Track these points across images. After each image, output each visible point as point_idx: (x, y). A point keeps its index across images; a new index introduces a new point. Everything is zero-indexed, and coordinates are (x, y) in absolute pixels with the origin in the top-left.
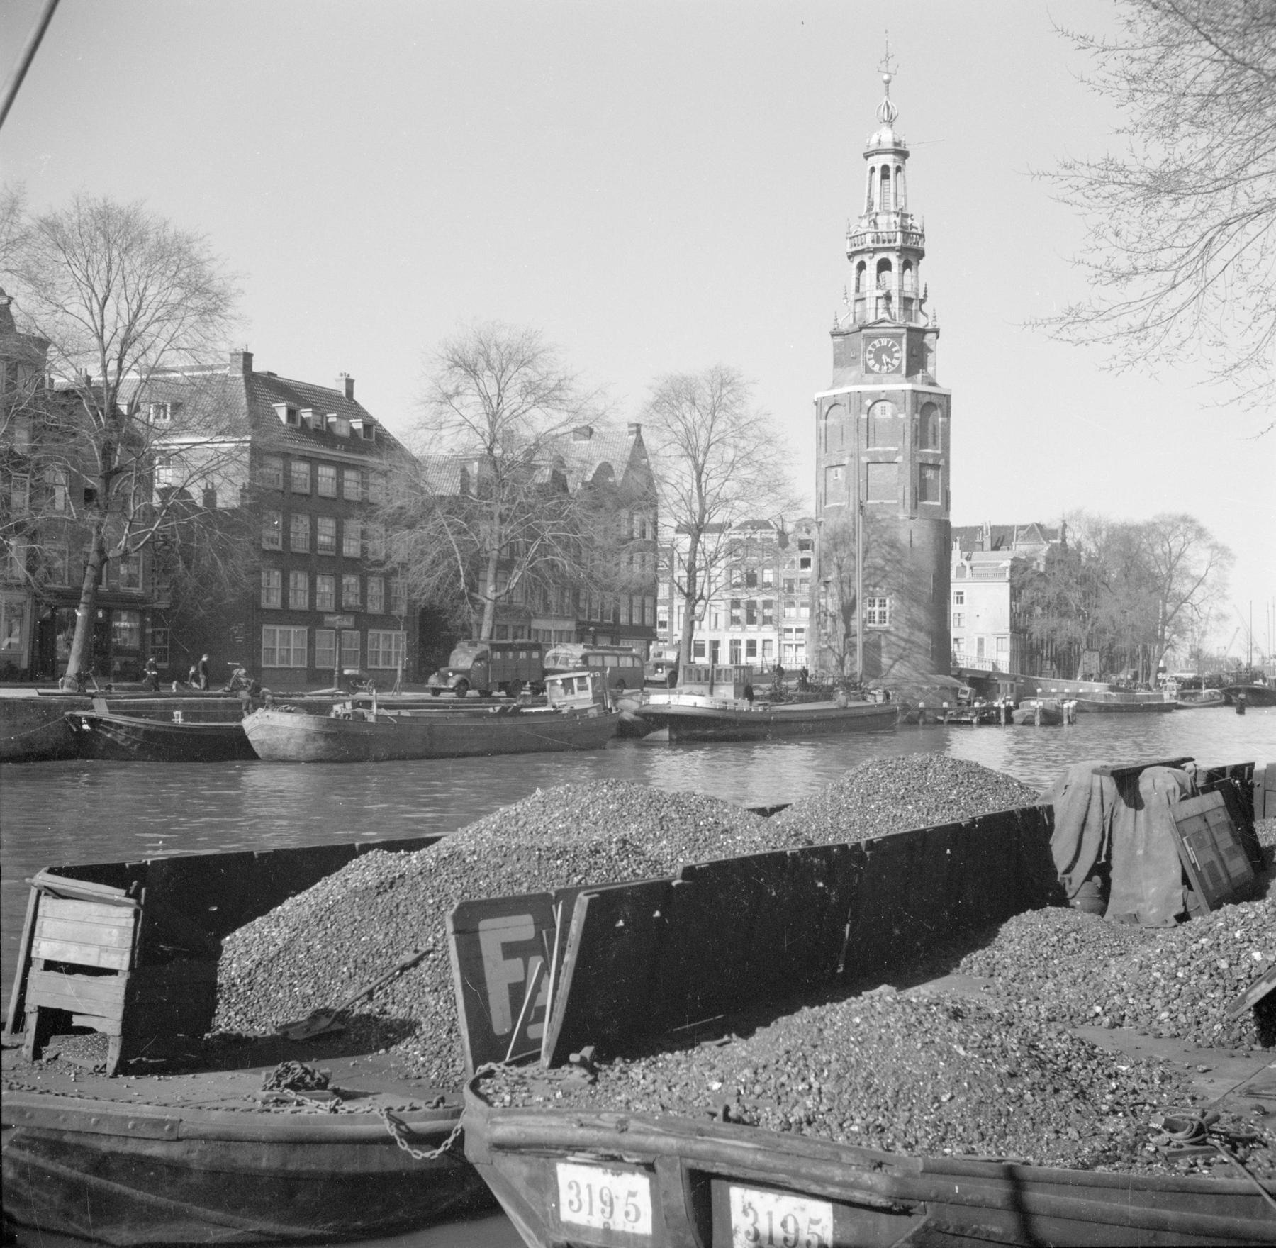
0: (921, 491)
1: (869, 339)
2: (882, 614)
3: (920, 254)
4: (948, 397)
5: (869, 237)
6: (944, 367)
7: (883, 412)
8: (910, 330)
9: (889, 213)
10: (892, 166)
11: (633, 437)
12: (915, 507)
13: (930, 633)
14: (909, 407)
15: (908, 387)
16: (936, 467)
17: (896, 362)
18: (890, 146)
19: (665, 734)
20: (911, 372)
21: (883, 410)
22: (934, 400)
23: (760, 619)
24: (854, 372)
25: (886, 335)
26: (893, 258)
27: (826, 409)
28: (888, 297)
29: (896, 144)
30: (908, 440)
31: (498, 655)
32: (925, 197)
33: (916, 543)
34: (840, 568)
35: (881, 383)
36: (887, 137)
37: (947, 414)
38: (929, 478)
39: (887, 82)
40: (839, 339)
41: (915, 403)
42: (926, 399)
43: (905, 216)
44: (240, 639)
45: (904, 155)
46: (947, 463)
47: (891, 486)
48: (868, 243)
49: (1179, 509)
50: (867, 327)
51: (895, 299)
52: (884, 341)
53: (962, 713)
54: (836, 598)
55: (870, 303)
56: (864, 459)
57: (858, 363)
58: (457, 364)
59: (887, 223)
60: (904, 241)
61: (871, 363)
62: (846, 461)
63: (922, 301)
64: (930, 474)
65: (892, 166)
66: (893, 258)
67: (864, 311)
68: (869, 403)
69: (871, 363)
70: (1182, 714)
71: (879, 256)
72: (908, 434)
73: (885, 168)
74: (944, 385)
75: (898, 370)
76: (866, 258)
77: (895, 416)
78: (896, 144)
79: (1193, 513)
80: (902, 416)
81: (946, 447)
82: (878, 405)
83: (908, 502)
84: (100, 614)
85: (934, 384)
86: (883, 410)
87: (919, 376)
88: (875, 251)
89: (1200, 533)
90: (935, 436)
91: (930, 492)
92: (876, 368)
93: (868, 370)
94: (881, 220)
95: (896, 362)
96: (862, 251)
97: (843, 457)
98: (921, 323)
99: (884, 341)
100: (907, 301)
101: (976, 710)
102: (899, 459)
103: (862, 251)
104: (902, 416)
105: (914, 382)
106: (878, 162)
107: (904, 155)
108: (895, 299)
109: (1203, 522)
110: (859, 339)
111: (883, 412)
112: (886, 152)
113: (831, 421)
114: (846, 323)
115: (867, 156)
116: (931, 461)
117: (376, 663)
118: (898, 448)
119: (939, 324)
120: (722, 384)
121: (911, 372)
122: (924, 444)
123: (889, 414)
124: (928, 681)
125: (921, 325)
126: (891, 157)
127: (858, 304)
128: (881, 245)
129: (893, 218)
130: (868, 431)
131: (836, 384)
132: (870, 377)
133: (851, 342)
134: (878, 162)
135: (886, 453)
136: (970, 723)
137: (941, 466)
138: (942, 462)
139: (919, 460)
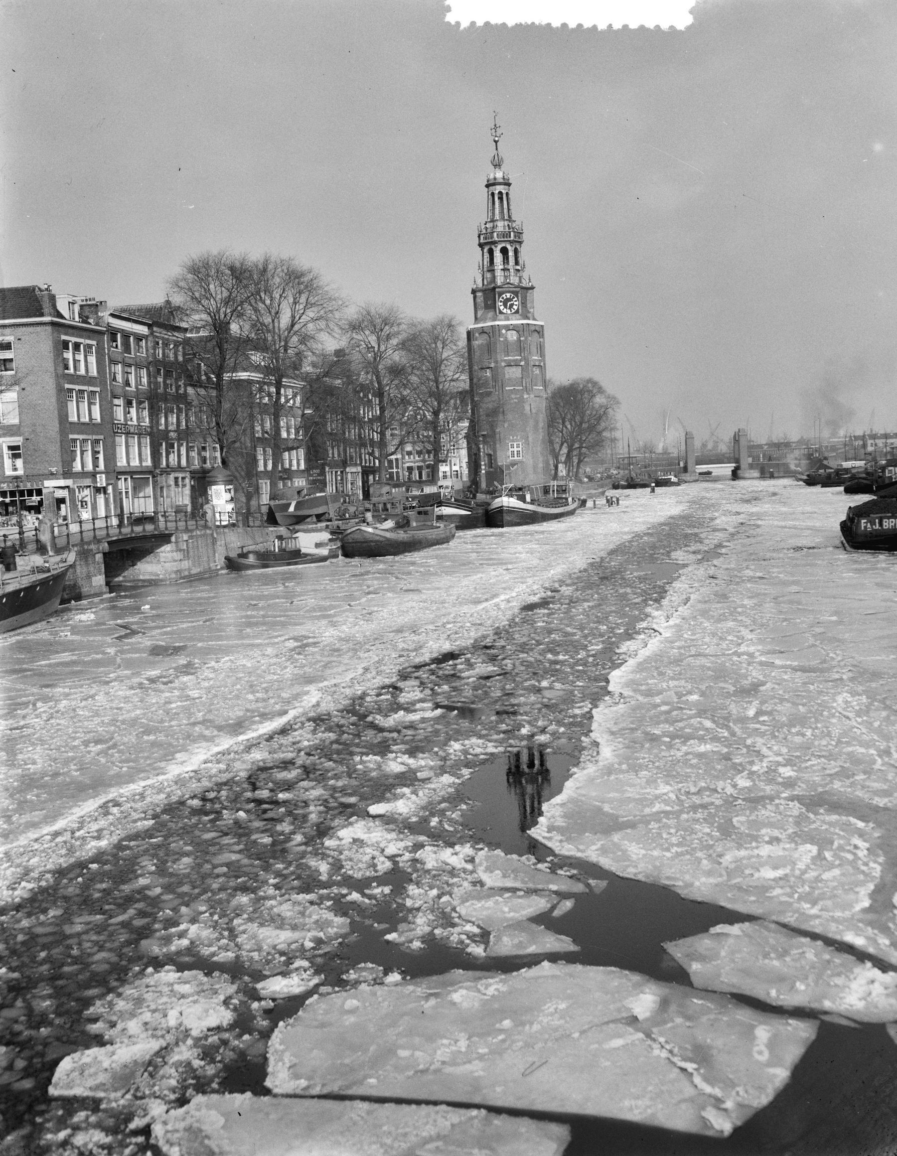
1: (500, 294)
2: (518, 452)
45: (509, 185)
52: (508, 295)
55: (499, 274)
56: (503, 364)
62: (492, 365)
71: (503, 245)
81: (542, 355)
99: (508, 295)
107: (509, 185)
112: (500, 184)
132: (502, 316)
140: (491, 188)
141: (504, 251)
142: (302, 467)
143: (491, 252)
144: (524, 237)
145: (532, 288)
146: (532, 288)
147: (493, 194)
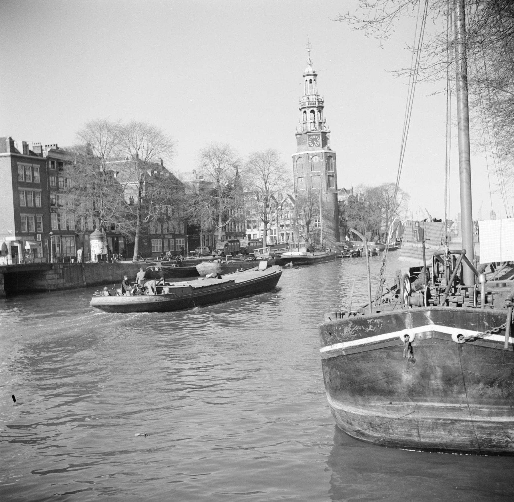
0: (329, 185)
1: (309, 136)
3: (323, 107)
4: (335, 153)
5: (307, 103)
7: (316, 160)
8: (322, 132)
9: (313, 95)
10: (313, 79)
13: (334, 230)
14: (324, 158)
15: (323, 151)
16: (333, 176)
17: (318, 143)
18: (312, 73)
19: (291, 264)
21: (316, 159)
22: (331, 155)
23: (252, 227)
24: (305, 147)
25: (315, 135)
28: (314, 122)
29: (314, 72)
30: (324, 168)
31: (230, 244)
32: (323, 89)
33: (328, 201)
34: (304, 210)
35: (314, 150)
36: (310, 70)
37: (335, 159)
38: (331, 179)
39: (309, 52)
42: (328, 155)
44: (146, 244)
45: (316, 75)
46: (336, 175)
47: (319, 184)
48: (307, 105)
52: (314, 137)
53: (346, 254)
54: (304, 220)
55: (309, 124)
56: (311, 175)
57: (306, 144)
58: (206, 156)
59: (312, 99)
60: (319, 104)
62: (305, 176)
63: (324, 123)
64: (331, 179)
67: (307, 127)
68: (311, 157)
69: (310, 144)
71: (312, 109)
72: (324, 166)
73: (311, 80)
75: (319, 146)
76: (306, 110)
77: (319, 161)
78: (314, 72)
80: (322, 161)
81: (335, 170)
83: (325, 188)
84: (115, 239)
85: (330, 150)
86: (316, 159)
87: (326, 147)
88: (309, 107)
91: (331, 184)
92: (312, 145)
93: (310, 146)
96: (305, 108)
97: (303, 175)
98: (324, 130)
99: (314, 137)
101: (351, 253)
102: (322, 174)
103: (305, 108)
104: (322, 161)
105: (324, 149)
106: (308, 78)
107: (316, 75)
110: (306, 135)
112: (311, 75)
113: (298, 163)
115: (304, 76)
116: (331, 175)
117: (157, 250)
119: (331, 130)
120: (272, 155)
122: (329, 170)
123: (318, 160)
124: (334, 245)
125: (324, 131)
126: (312, 76)
128: (311, 106)
129: (314, 96)
131: (299, 151)
132: (310, 148)
133: (301, 137)
134: (308, 78)
135: (318, 173)
136: (349, 257)
137: (334, 176)
138: (334, 175)
140: (306, 78)
141: (313, 112)
142: (182, 232)
143: (305, 112)
144: (324, 104)
145: (329, 133)
147: (306, 81)
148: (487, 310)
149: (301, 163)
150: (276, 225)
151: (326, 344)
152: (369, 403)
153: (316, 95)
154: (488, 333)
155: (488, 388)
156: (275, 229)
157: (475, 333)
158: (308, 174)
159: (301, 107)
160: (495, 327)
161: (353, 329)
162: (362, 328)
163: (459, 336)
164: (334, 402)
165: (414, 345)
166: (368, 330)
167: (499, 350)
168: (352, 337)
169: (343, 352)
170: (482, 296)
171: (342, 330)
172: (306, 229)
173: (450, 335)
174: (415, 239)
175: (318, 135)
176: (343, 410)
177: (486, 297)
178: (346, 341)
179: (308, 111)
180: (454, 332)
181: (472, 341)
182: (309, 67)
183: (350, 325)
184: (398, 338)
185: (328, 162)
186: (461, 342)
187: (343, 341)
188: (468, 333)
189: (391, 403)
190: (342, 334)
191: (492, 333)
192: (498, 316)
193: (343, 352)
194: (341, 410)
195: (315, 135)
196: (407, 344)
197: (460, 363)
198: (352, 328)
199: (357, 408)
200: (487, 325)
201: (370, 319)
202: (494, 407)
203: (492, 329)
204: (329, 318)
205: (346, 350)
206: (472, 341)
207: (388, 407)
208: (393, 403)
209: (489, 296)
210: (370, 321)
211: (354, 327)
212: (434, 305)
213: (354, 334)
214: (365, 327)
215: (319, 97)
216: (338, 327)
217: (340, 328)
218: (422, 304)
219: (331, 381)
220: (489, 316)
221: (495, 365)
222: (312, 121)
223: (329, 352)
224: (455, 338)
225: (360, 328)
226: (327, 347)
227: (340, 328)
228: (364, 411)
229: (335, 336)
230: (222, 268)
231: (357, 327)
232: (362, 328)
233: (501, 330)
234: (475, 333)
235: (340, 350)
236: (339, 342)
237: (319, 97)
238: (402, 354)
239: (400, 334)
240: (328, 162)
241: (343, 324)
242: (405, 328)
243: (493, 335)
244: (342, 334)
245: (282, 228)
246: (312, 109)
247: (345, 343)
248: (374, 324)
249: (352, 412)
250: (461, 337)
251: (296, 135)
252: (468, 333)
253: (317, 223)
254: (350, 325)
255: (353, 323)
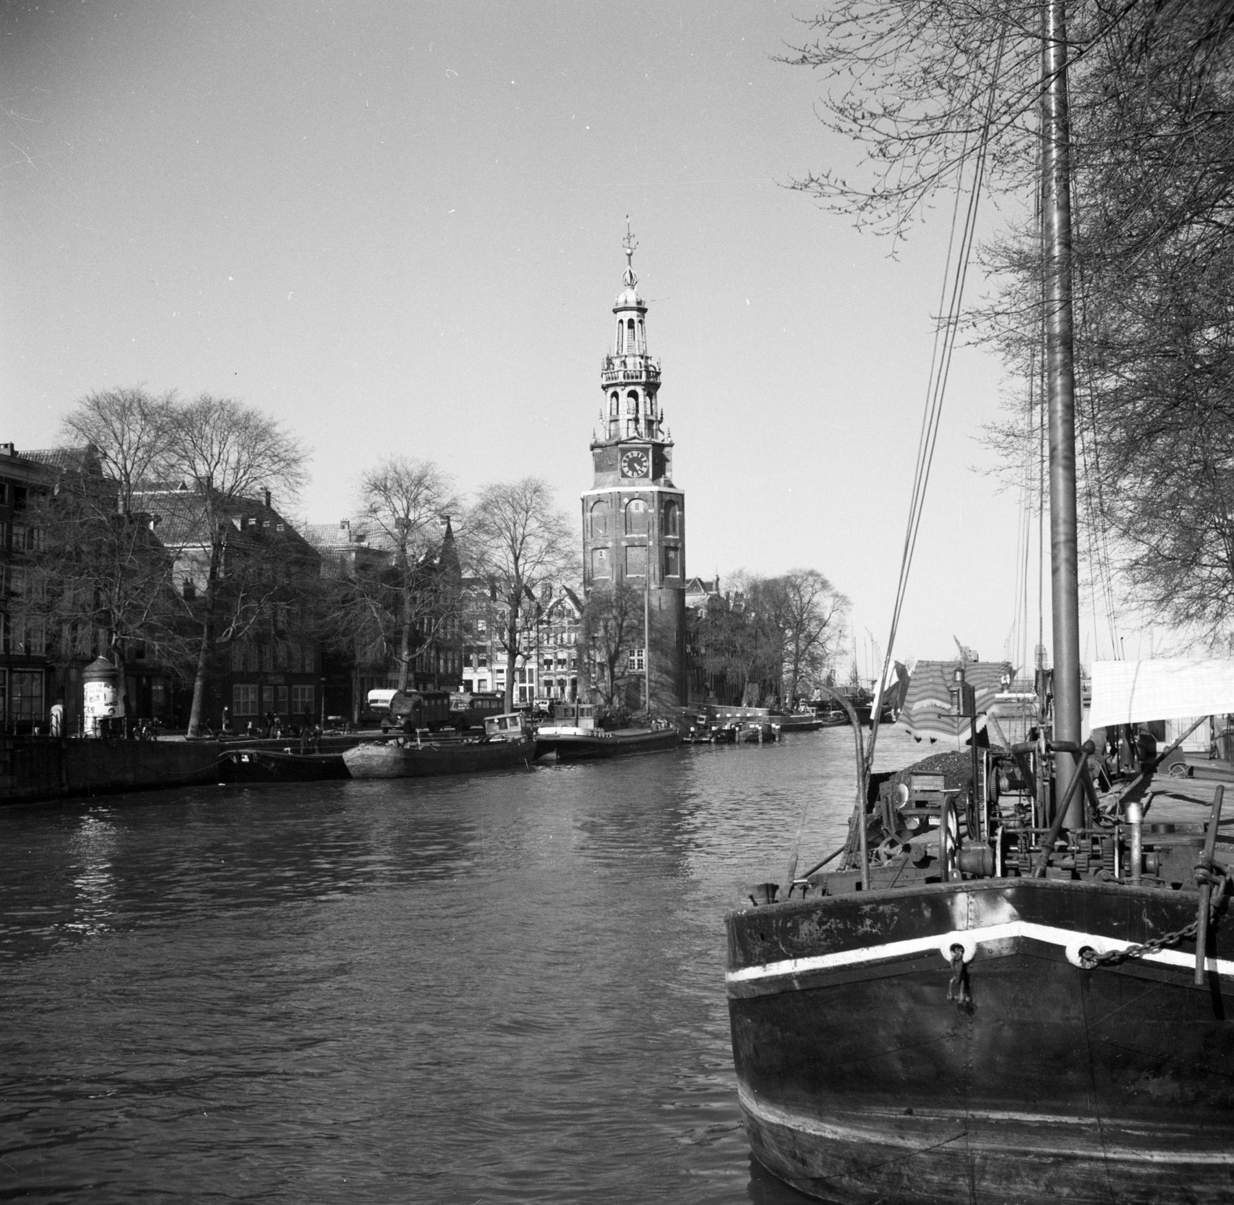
0: (666, 567)
1: (624, 451)
3: (657, 386)
4: (682, 496)
5: (621, 374)
6: (679, 474)
7: (637, 508)
8: (655, 445)
9: (635, 356)
10: (636, 319)
11: (444, 527)
12: (662, 580)
14: (656, 504)
15: (656, 489)
16: (675, 549)
17: (645, 470)
18: (634, 305)
20: (656, 477)
21: (637, 506)
22: (674, 498)
23: (475, 663)
24: (612, 476)
25: (637, 449)
26: (639, 390)
27: (591, 504)
28: (637, 420)
30: (656, 529)
31: (426, 703)
32: (661, 344)
33: (664, 607)
34: (606, 627)
35: (634, 485)
36: (631, 297)
37: (682, 509)
38: (671, 554)
39: (630, 255)
40: (598, 451)
41: (661, 501)
42: (667, 498)
43: (647, 358)
46: (683, 545)
47: (643, 565)
48: (621, 379)
49: (808, 567)
50: (622, 443)
51: (642, 421)
52: (635, 453)
53: (703, 735)
55: (623, 424)
56: (624, 544)
57: (615, 469)
58: (376, 487)
59: (633, 364)
60: (648, 377)
61: (626, 469)
62: (610, 545)
63: (660, 422)
64: (672, 554)
65: (636, 319)
66: (639, 390)
67: (618, 429)
68: (626, 500)
69: (626, 469)
70: (825, 730)
71: (632, 388)
72: (656, 525)
73: (631, 323)
74: (680, 486)
75: (646, 475)
76: (618, 389)
77: (646, 511)
78: (639, 303)
79: (819, 570)
80: (651, 511)
81: (682, 534)
82: (633, 502)
84: (144, 681)
85: (671, 486)
86: (637, 506)
87: (662, 480)
88: (626, 384)
89: (825, 585)
90: (674, 526)
92: (630, 474)
93: (624, 475)
94: (629, 361)
95: (645, 470)
96: (616, 385)
98: (660, 439)
99: (635, 453)
100: (650, 423)
101: (714, 733)
102: (651, 543)
103: (616, 385)
104: (651, 511)
105: (658, 484)
106: (626, 316)
108: (642, 421)
109: (826, 576)
110: (615, 451)
111: (637, 508)
112: (631, 309)
113: (595, 513)
114: (602, 438)
115: (615, 311)
116: (672, 545)
117: (246, 711)
118: (649, 536)
119: (674, 439)
120: (536, 491)
121: (656, 477)
122: (667, 533)
123: (641, 510)
125: (659, 441)
127: (613, 425)
129: (638, 359)
130: (627, 522)
131: (597, 485)
132: (625, 481)
133: (606, 455)
134: (626, 316)
135: (641, 539)
137: (679, 547)
138: (680, 545)
139: (664, 544)
140: (619, 314)
141: (633, 394)
143: (615, 395)
144: (662, 379)
145: (671, 445)
146: (671, 445)
147: (621, 321)
148: (1150, 889)
149: (601, 514)
150: (534, 659)
151: (748, 963)
152: (855, 1109)
153: (642, 357)
154: (1152, 944)
155: (1147, 1078)
156: (531, 671)
157: (1121, 946)
158: (617, 541)
159: (605, 383)
160: (1168, 931)
161: (824, 927)
162: (845, 924)
163: (1084, 951)
164: (762, 1106)
165: (969, 970)
166: (861, 930)
167: (1177, 986)
168: (820, 946)
169: (796, 983)
170: (1136, 854)
171: (795, 929)
172: (607, 673)
173: (1061, 949)
174: (955, 711)
175: (645, 451)
176: (783, 1127)
177: (1143, 859)
178: (802, 956)
179: (623, 394)
180: (1072, 942)
181: (1114, 963)
182: (629, 289)
183: (815, 917)
184: (935, 953)
185: (666, 515)
186: (1088, 965)
187: (796, 956)
188: (1105, 945)
189: (909, 1112)
190: (795, 939)
191: (1164, 946)
192: (1176, 905)
193: (796, 983)
194: (778, 1126)
195: (637, 449)
196: (958, 968)
197: (1082, 1016)
198: (820, 923)
199: (822, 1120)
200: (1151, 924)
201: (867, 903)
202: (1161, 1125)
203: (1162, 937)
204: (751, 897)
205: (804, 976)
206: (1114, 963)
207: (901, 1120)
208: (914, 1111)
209: (1150, 854)
210: (867, 908)
211: (825, 923)
212: (1018, 874)
213: (825, 940)
214: (855, 923)
215: (650, 362)
216: (785, 923)
217: (789, 925)
218: (989, 870)
219: (756, 1051)
220: (1155, 904)
221: (1167, 1024)
222: (631, 416)
223: (757, 982)
224: (1073, 957)
225: (841, 926)
226: (751, 969)
227: (789, 925)
228: (840, 1130)
229: (776, 944)
230: (405, 760)
231: (833, 923)
232: (845, 924)
233: (1182, 938)
234: (1121, 946)
235: (787, 978)
236: (786, 957)
237: (650, 362)
238: (947, 993)
239: (941, 942)
240: (666, 515)
241: (796, 914)
242: (954, 929)
243: (1165, 951)
244: (795, 939)
245: (549, 668)
246: (632, 388)
247: (800, 961)
248: (877, 917)
249: (810, 1131)
250: (1087, 954)
251: (593, 448)
252: (1105, 945)
253: (635, 658)
254: (815, 917)
255: (824, 911)
